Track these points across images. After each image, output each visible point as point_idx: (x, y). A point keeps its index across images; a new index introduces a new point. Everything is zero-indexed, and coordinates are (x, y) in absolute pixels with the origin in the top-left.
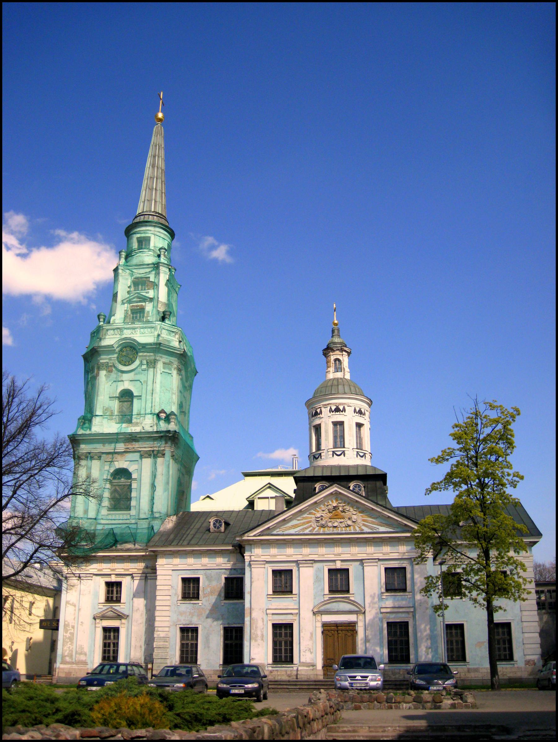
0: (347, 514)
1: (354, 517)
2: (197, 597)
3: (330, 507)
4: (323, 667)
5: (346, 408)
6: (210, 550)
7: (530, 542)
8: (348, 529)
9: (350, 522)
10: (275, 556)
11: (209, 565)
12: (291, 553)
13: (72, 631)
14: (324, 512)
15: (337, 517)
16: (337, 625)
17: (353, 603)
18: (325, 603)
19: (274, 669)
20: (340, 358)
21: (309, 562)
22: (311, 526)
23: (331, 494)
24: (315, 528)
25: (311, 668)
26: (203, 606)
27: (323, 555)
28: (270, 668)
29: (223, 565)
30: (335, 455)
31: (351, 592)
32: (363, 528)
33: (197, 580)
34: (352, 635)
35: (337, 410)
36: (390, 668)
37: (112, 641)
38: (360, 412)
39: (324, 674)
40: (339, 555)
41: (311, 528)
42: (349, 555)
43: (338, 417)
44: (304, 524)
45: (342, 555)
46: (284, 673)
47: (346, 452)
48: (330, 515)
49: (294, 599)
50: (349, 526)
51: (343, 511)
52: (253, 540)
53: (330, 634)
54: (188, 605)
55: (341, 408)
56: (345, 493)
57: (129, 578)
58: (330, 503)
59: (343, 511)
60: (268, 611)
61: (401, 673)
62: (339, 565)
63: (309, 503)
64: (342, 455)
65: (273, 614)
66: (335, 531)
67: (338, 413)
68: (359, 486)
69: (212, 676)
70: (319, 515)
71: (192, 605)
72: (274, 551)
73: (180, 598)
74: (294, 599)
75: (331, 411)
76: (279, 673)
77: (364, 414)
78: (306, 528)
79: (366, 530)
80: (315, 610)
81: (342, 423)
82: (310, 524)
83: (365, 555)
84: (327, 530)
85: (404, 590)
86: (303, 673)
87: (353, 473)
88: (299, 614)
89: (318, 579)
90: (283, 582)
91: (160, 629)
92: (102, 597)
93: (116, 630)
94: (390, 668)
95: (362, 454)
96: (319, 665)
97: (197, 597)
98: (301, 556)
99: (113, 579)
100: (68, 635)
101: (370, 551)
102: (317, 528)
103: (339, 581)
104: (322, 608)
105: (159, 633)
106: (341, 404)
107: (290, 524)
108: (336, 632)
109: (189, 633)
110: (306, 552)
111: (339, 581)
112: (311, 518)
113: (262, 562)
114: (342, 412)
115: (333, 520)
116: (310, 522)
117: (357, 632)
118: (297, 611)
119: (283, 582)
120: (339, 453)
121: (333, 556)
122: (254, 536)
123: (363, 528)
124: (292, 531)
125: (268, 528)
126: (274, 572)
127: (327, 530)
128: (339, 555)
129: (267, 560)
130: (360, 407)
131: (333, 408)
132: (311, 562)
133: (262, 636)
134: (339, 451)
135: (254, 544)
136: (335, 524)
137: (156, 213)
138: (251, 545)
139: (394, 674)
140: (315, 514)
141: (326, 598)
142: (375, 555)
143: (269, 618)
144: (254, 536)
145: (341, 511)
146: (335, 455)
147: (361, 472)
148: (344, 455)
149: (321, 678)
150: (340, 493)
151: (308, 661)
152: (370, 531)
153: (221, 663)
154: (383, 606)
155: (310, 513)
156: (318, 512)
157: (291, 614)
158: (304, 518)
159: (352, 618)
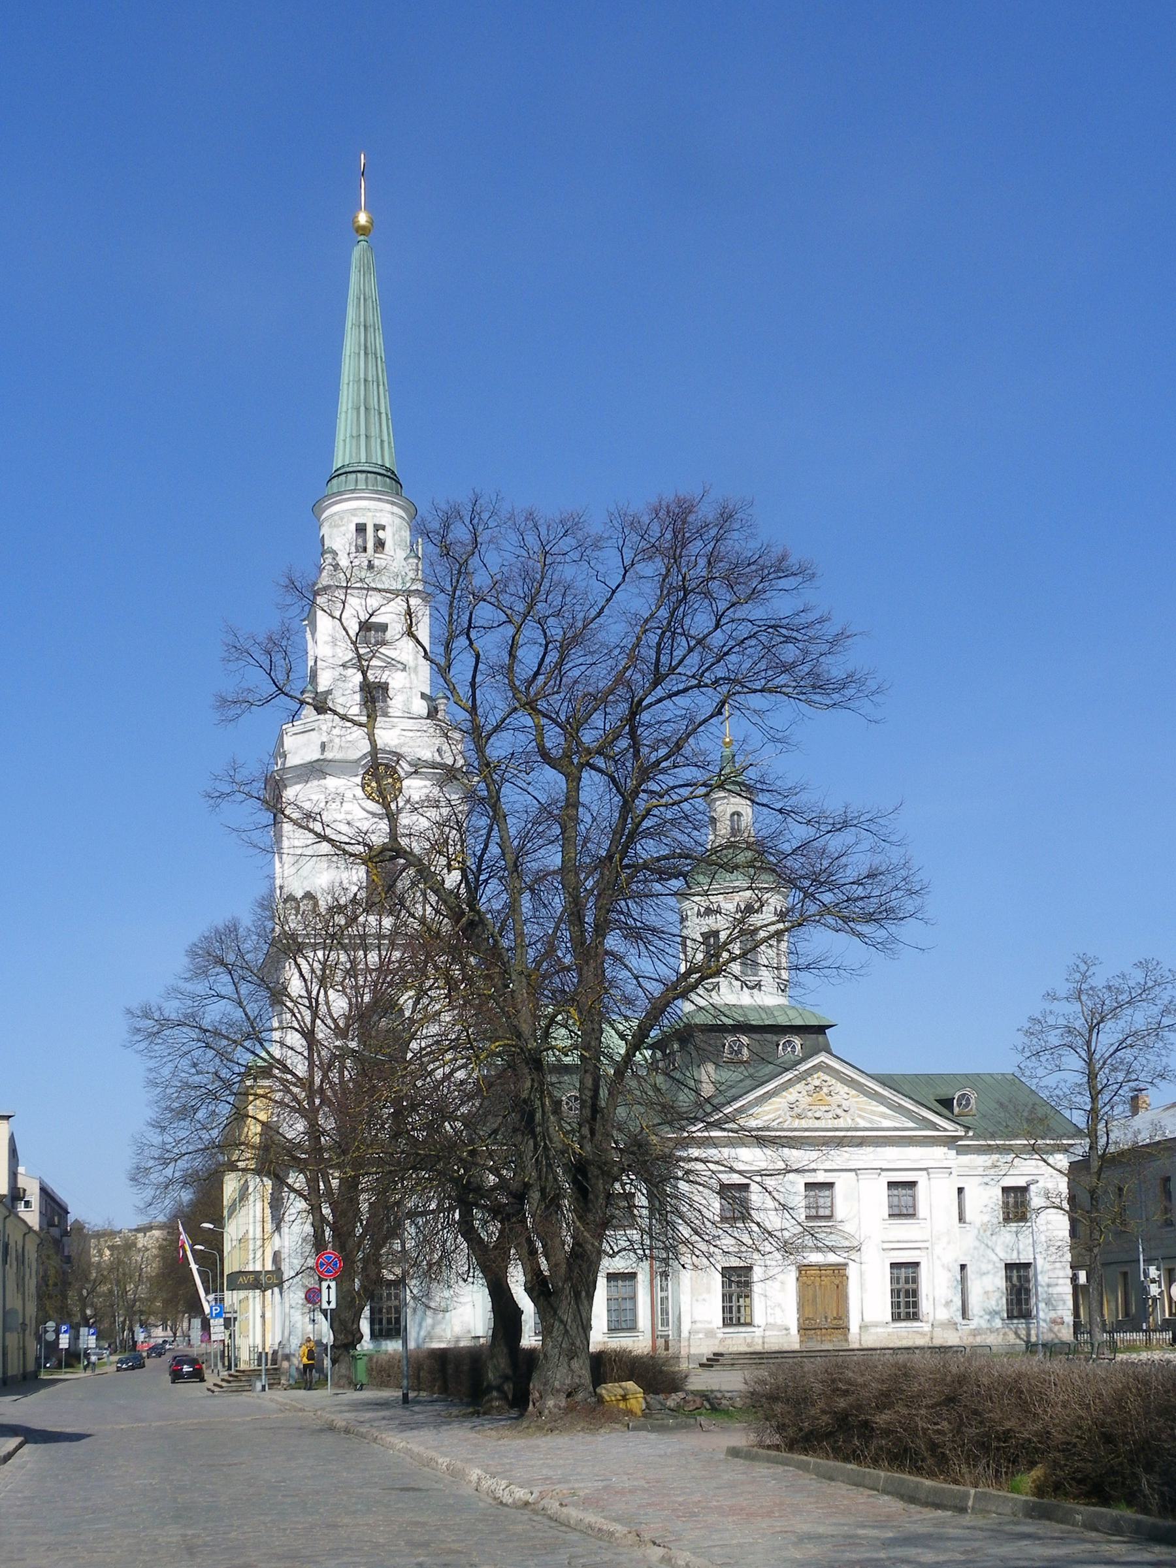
0: (836, 1099)
9: (839, 1112)
25: (784, 1332)
32: (858, 1120)
39: (801, 1342)
46: (742, 1341)
53: (809, 1282)
62: (821, 1177)
66: (817, 1124)
79: (862, 1123)
84: (804, 1124)
86: (773, 1340)
96: (794, 1330)
123: (858, 1120)
149: (797, 1347)
151: (779, 1322)
152: (868, 1125)
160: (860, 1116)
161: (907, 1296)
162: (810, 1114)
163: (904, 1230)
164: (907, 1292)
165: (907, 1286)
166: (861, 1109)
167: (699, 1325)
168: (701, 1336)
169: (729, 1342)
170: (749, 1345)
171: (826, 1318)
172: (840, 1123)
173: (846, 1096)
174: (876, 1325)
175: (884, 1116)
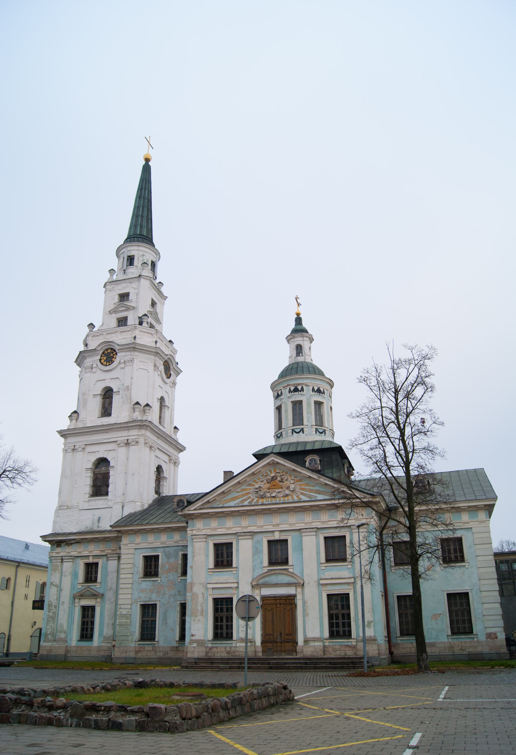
0: (286, 483)
1: (292, 486)
2: (156, 575)
3: (268, 477)
4: (262, 643)
5: (305, 388)
6: (168, 528)
7: (485, 505)
8: (286, 498)
9: (287, 492)
10: (216, 529)
11: (167, 543)
12: (230, 526)
13: (54, 611)
14: (263, 483)
15: (275, 487)
16: (275, 598)
17: (292, 575)
18: (263, 576)
19: (214, 645)
20: (301, 343)
21: (247, 534)
22: (250, 498)
23: (269, 464)
24: (253, 500)
26: (162, 583)
27: (262, 527)
28: (210, 645)
29: (180, 542)
30: (294, 433)
31: (290, 563)
33: (157, 557)
34: (291, 609)
35: (296, 390)
36: (331, 644)
37: (89, 620)
38: (319, 391)
39: (263, 651)
40: (277, 526)
41: (250, 500)
42: (287, 526)
43: (297, 397)
44: (244, 495)
45: (281, 526)
46: (223, 650)
47: (304, 429)
48: (268, 485)
49: (234, 572)
50: (287, 495)
51: (282, 481)
52: (193, 514)
54: (148, 583)
55: (299, 388)
56: (282, 462)
57: (105, 559)
58: (269, 473)
59: (282, 481)
60: (209, 586)
61: (342, 649)
62: (277, 536)
63: (247, 475)
64: (301, 433)
65: (213, 589)
67: (297, 393)
68: (315, 460)
69: (169, 652)
70: (257, 486)
71: (152, 582)
72: (214, 523)
73: (141, 575)
74: (234, 572)
75: (290, 391)
76: (218, 650)
77: (324, 393)
78: (245, 500)
79: (304, 498)
80: (254, 583)
81: (300, 402)
82: (249, 495)
83: (303, 525)
85: (344, 560)
87: (309, 447)
88: (237, 587)
89: (256, 551)
90: (223, 556)
91: (122, 606)
92: (81, 577)
93: (93, 608)
94: (331, 644)
95: (321, 431)
97: (156, 575)
98: (240, 528)
99: (91, 560)
100: (51, 614)
101: (307, 520)
102: (256, 499)
103: (278, 553)
104: (261, 581)
105: (121, 610)
106: (299, 384)
107: (229, 497)
108: (275, 606)
109: (148, 610)
110: (246, 524)
111: (278, 553)
112: (250, 489)
113: (203, 536)
114: (300, 391)
115: (271, 491)
116: (249, 493)
117: (296, 606)
118: (236, 585)
119: (223, 556)
120: (297, 431)
121: (271, 527)
122: (195, 510)
124: (232, 504)
125: (208, 502)
126: (216, 545)
127: (265, 501)
128: (277, 525)
129: (208, 534)
130: (319, 386)
131: (292, 389)
132: (249, 534)
133: (202, 610)
134: (298, 428)
135: (196, 518)
136: (273, 495)
137: (141, 235)
138: (193, 519)
139: (335, 650)
140: (253, 485)
141: (265, 570)
142: (313, 524)
143: (209, 593)
144: (195, 510)
145: (280, 481)
146: (294, 433)
147: (317, 446)
148: (303, 432)
150: (278, 463)
152: (308, 499)
153: (178, 639)
154: (323, 578)
155: (250, 485)
156: (257, 483)
157: (231, 588)
158: (243, 489)
159: (291, 591)
160: (302, 494)
161: (343, 618)
162: (268, 495)
163: (340, 572)
164: (343, 615)
165: (343, 612)
166: (302, 489)
167: (194, 638)
168: (195, 645)
169: (215, 650)
170: (228, 653)
171: (281, 634)
172: (290, 499)
173: (292, 482)
174: (314, 640)
175: (318, 492)
